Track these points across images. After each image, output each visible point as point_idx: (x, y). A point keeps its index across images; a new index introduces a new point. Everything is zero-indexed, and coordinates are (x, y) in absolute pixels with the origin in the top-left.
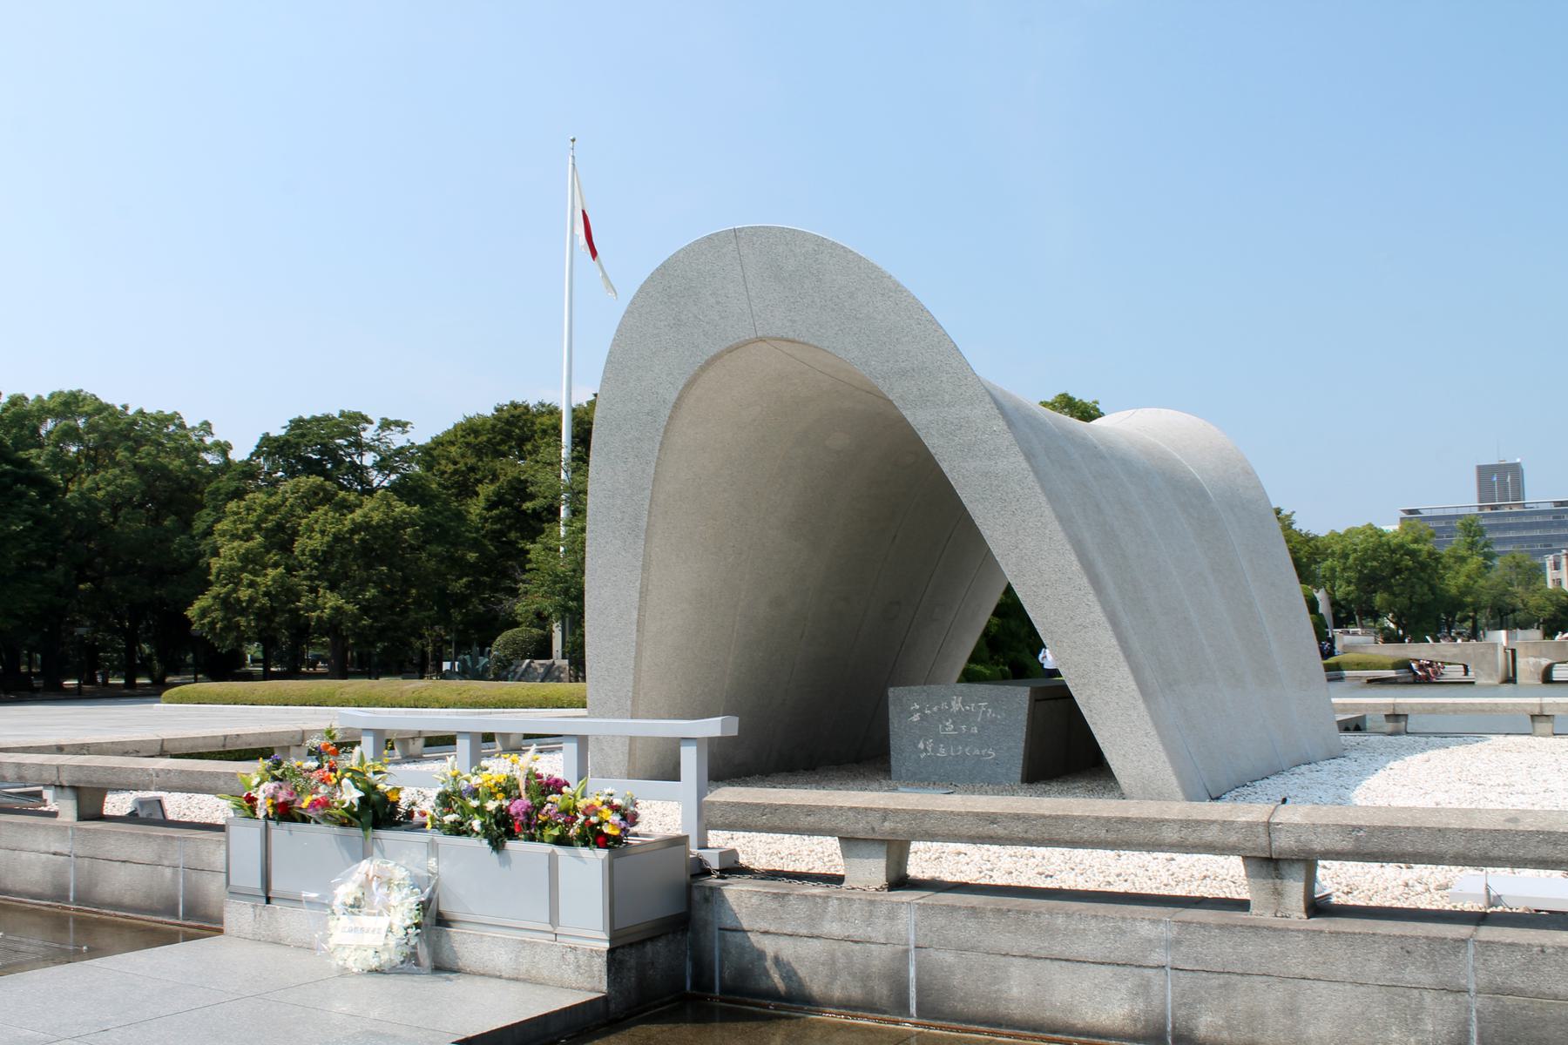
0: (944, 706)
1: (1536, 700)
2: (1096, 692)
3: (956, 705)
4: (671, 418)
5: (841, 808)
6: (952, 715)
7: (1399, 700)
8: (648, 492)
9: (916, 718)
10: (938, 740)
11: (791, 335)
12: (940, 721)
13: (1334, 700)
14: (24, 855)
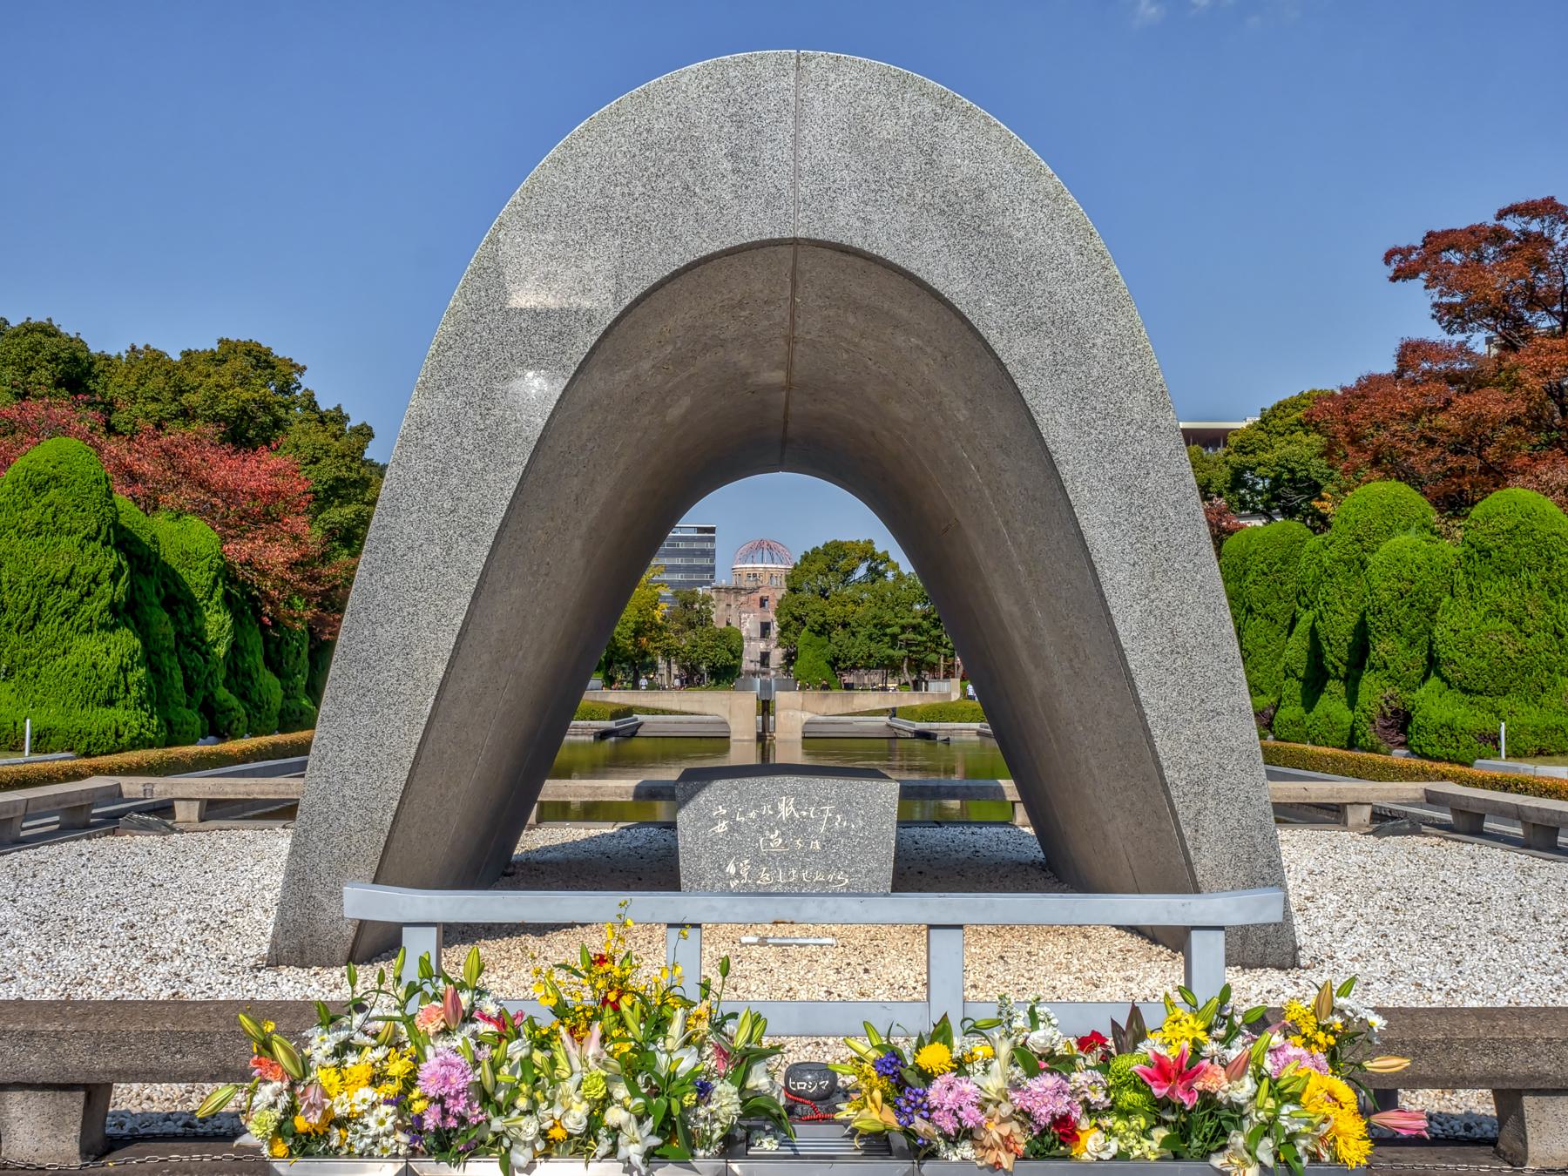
0: (766, 810)
2: (1211, 804)
3: (785, 809)
4: (593, 349)
5: (1549, 1041)
6: (779, 824)
8: (518, 470)
9: (722, 827)
10: (758, 860)
11: (858, 242)
12: (760, 831)
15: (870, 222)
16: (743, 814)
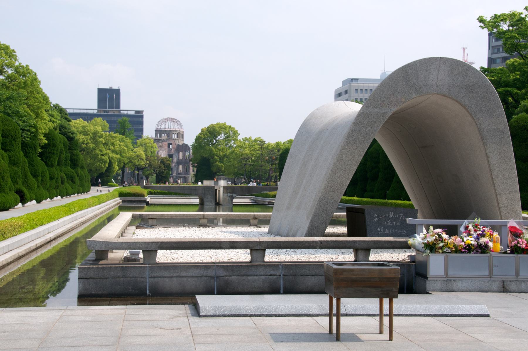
1: (252, 213)
3: (391, 215)
6: (390, 219)
7: (256, 213)
9: (376, 219)
10: (385, 228)
13: (335, 214)
14: (249, 278)
15: (450, 90)
16: (381, 216)
